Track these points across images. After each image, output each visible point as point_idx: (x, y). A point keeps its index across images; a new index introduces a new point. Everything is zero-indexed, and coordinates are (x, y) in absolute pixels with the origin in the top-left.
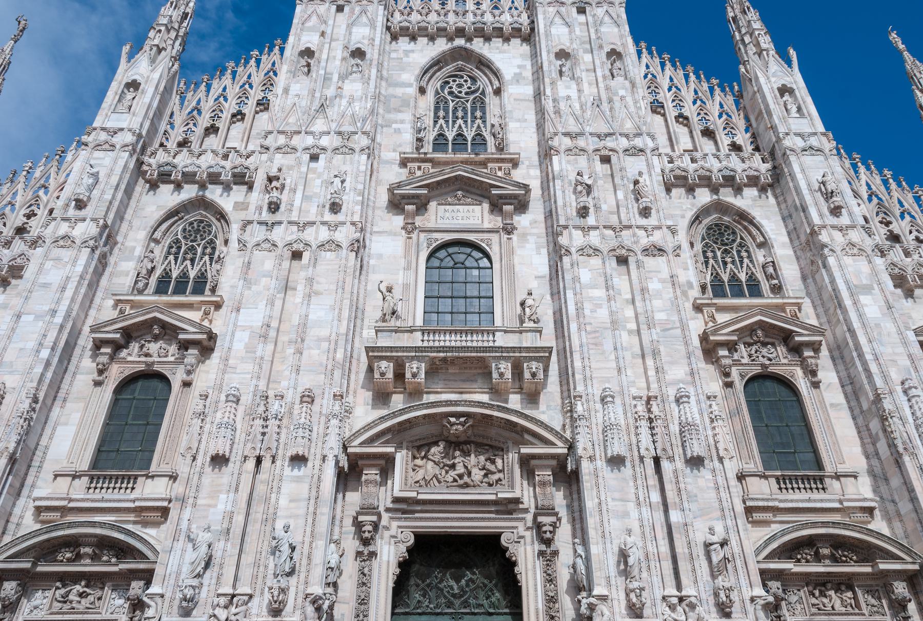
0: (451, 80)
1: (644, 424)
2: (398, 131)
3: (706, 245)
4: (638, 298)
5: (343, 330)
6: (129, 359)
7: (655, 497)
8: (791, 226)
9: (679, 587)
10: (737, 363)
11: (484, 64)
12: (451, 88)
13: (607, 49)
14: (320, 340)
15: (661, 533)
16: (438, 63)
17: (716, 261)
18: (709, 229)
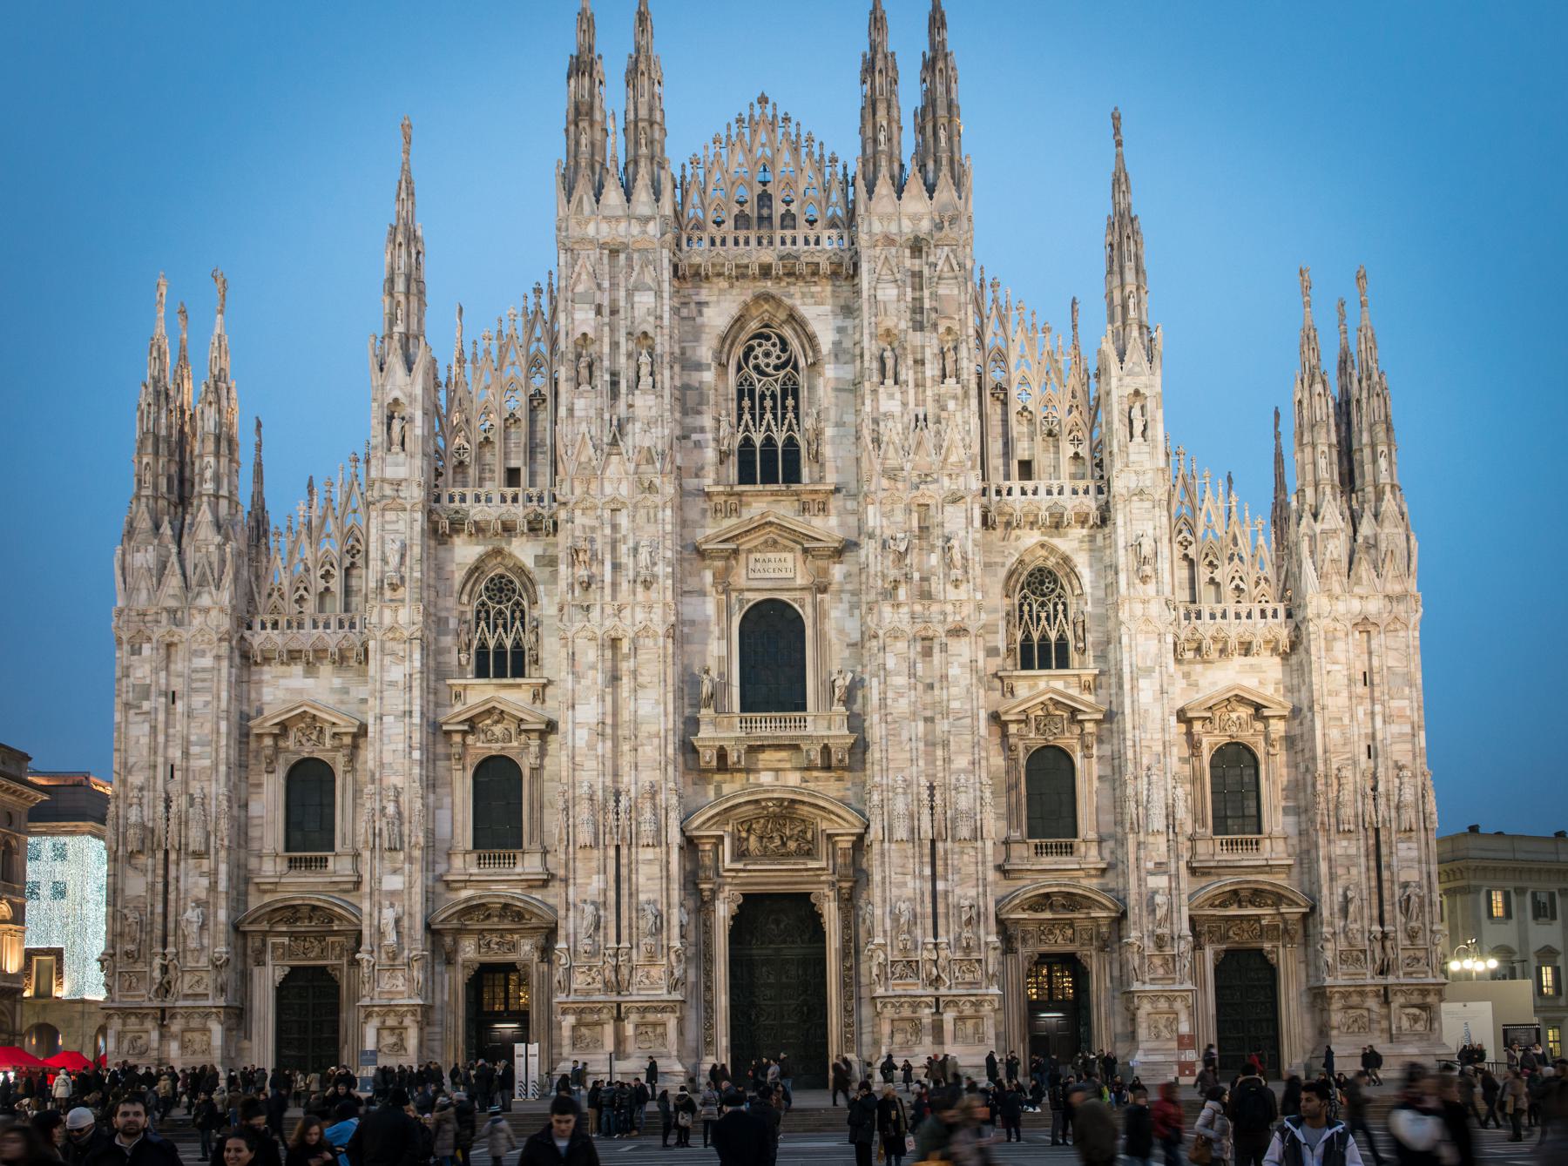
0: (755, 342)
1: (926, 812)
2: (698, 444)
3: (1025, 597)
4: (937, 685)
5: (670, 725)
6: (479, 744)
7: (927, 871)
8: (1109, 580)
9: (936, 936)
10: (1021, 737)
11: (793, 318)
12: (756, 358)
14: (650, 736)
15: (928, 899)
16: (739, 321)
17: (1031, 617)
18: (1031, 575)
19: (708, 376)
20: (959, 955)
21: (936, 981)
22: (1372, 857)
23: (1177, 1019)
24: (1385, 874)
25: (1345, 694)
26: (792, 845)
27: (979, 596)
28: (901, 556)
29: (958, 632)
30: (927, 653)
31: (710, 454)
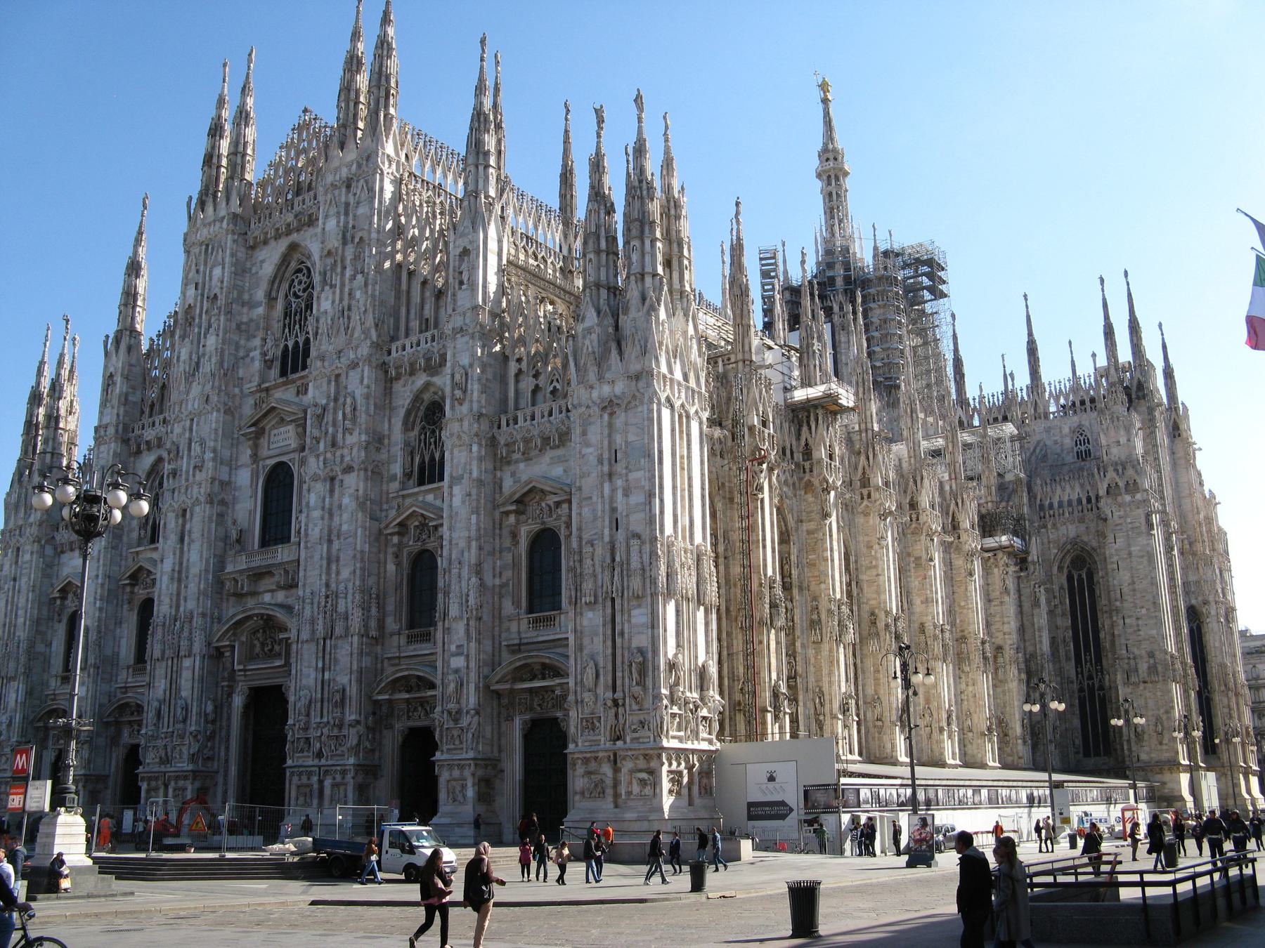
3: (424, 428)
7: (320, 665)
13: (357, 240)
18: (428, 408)
19: (261, 310)
20: (335, 732)
21: (319, 755)
22: (609, 627)
23: (464, 787)
24: (618, 640)
25: (594, 474)
26: (277, 648)
27: (363, 438)
28: (320, 418)
29: (348, 469)
30: (332, 491)
31: (257, 364)
